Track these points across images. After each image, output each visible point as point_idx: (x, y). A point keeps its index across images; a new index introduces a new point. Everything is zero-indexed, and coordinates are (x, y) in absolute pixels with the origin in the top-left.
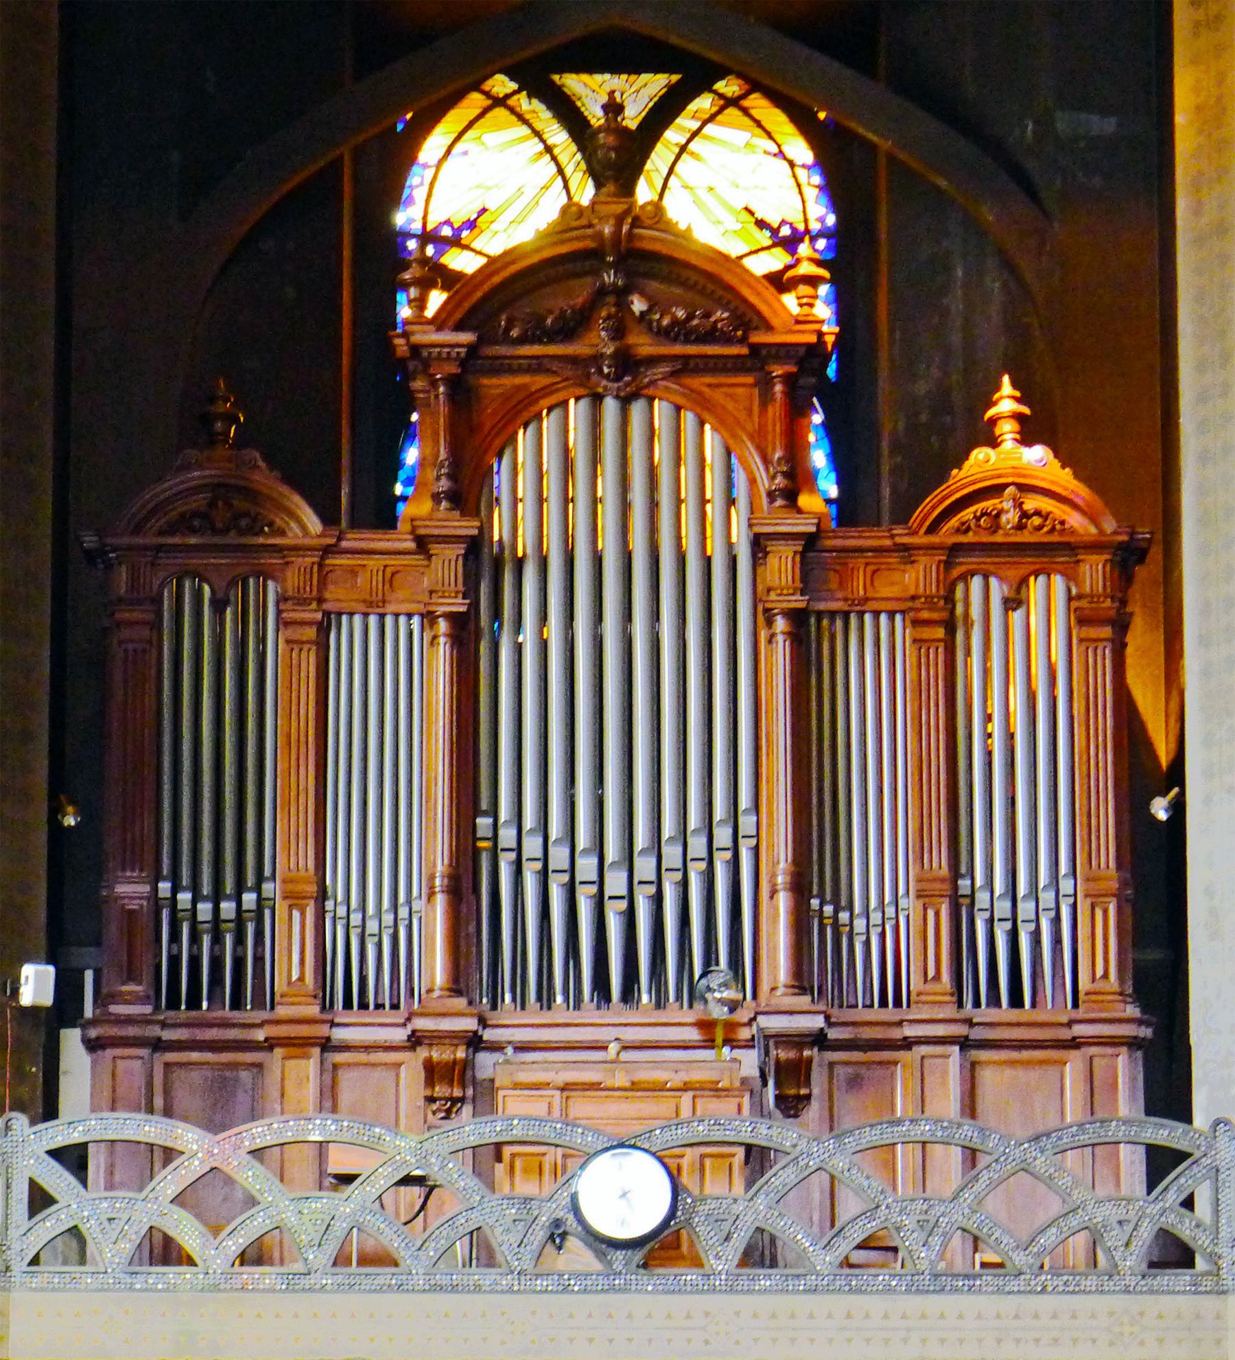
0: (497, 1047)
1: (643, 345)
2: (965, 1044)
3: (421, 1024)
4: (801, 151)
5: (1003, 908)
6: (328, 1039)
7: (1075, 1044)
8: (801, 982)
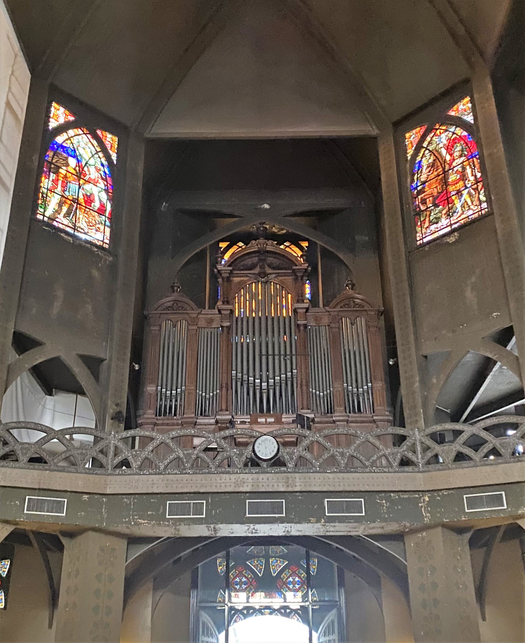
2: (347, 421)
3: (218, 417)
6: (196, 422)
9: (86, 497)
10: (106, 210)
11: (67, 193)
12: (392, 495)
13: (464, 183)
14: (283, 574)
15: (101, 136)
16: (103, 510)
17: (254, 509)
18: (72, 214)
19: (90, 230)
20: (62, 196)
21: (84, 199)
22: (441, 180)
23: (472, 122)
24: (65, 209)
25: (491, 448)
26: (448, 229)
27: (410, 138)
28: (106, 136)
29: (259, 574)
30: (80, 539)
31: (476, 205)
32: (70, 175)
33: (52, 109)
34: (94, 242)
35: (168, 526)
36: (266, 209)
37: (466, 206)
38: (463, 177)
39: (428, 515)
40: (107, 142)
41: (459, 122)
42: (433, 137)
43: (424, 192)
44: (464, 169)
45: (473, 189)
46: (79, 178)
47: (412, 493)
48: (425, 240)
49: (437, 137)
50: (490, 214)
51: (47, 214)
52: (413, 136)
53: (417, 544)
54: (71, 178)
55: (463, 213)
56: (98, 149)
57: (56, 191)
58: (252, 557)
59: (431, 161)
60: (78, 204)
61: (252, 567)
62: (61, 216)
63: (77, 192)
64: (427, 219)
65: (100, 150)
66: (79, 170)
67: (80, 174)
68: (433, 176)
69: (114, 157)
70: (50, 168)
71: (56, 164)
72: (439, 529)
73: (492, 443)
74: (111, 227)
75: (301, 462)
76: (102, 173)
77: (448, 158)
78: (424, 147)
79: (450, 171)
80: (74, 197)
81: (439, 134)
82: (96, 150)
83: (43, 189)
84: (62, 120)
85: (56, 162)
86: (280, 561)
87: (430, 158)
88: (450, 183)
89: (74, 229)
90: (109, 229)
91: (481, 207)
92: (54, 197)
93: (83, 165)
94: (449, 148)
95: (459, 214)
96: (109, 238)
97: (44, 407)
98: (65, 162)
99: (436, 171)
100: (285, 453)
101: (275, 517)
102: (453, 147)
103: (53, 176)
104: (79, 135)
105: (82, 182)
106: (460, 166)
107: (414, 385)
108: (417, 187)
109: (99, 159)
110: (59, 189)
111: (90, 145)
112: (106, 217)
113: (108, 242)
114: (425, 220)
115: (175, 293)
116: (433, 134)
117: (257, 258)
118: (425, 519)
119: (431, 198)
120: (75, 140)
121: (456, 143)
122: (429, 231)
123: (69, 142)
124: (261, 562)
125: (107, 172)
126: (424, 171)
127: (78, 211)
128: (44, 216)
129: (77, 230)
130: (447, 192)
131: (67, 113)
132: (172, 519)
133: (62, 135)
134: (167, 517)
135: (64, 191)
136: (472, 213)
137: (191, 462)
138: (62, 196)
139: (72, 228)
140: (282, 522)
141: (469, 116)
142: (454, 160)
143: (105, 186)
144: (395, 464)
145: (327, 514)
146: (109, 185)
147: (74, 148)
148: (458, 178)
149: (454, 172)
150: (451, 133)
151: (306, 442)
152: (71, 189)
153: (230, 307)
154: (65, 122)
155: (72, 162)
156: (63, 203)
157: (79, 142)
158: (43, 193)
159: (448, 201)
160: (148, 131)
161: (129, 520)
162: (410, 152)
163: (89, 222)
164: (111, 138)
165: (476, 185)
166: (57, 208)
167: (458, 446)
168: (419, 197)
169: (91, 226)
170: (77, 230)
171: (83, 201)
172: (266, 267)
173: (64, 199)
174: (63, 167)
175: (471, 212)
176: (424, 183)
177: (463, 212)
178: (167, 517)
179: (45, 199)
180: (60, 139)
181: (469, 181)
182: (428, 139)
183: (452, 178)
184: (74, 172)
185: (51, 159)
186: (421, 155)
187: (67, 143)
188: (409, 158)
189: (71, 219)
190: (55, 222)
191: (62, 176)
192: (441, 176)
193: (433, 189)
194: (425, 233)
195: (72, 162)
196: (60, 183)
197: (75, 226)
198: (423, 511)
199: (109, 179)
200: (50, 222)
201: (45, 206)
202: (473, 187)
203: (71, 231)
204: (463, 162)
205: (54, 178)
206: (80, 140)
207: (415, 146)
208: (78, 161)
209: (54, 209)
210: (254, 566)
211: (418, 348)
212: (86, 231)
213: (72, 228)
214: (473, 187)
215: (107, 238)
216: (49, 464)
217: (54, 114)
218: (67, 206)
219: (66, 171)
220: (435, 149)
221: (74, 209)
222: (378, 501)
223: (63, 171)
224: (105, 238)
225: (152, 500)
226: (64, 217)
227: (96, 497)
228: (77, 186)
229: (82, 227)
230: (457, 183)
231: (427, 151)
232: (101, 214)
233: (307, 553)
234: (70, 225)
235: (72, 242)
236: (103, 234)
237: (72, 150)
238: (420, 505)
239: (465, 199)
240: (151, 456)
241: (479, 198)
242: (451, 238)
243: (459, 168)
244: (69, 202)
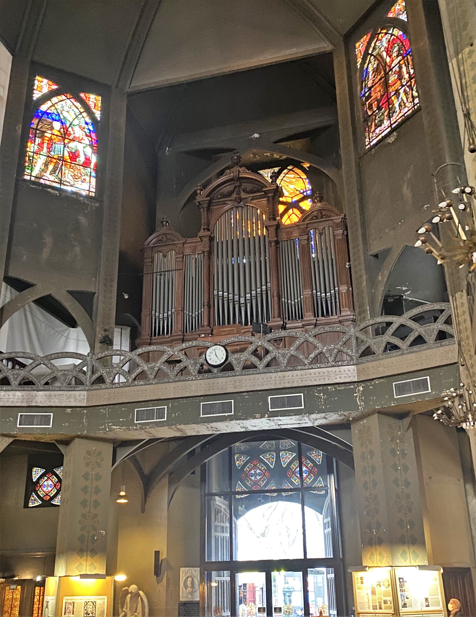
4: (304, 176)
9: (69, 410)
10: (90, 163)
11: (52, 153)
12: (329, 387)
13: (401, 82)
14: (292, 465)
15: (85, 98)
16: (84, 420)
17: (208, 409)
18: (58, 171)
19: (76, 182)
20: (48, 156)
21: (69, 156)
22: (383, 82)
23: (406, 20)
24: (51, 167)
25: (416, 336)
27: (359, 47)
28: (90, 98)
29: (271, 466)
30: (72, 446)
31: (410, 102)
32: (55, 137)
33: (36, 82)
34: (80, 192)
35: (136, 429)
36: (256, 138)
37: (402, 104)
38: (400, 77)
39: (362, 403)
40: (90, 103)
41: (396, 23)
42: (376, 42)
43: (372, 97)
44: (400, 68)
45: (408, 86)
46: (64, 138)
47: (348, 384)
48: (372, 144)
49: (379, 42)
50: (419, 109)
51: (34, 174)
52: (362, 44)
53: (360, 431)
54: (56, 139)
55: (400, 112)
56: (82, 110)
57: (42, 153)
58: (264, 451)
59: (375, 66)
60: (63, 161)
61: (265, 460)
63: (62, 151)
64: (373, 123)
65: (84, 110)
66: (64, 131)
68: (377, 80)
69: (98, 115)
70: (36, 133)
71: (41, 129)
72: (376, 415)
73: (417, 331)
74: (96, 177)
76: (87, 131)
77: (388, 60)
78: (370, 54)
79: (390, 73)
80: (60, 155)
81: (381, 38)
82: (80, 112)
83: (29, 153)
84: (45, 90)
85: (41, 128)
86: (289, 454)
87: (374, 64)
88: (390, 84)
89: (61, 184)
90: (95, 179)
91: (414, 103)
92: (40, 158)
93: (68, 127)
95: (397, 113)
96: (94, 187)
97: (67, 338)
98: (50, 126)
99: (380, 75)
100: (233, 359)
101: (225, 416)
102: (392, 47)
103: (38, 140)
104: (63, 100)
105: (66, 141)
106: (398, 65)
107: (362, 283)
109: (83, 119)
110: (45, 150)
111: (73, 108)
112: (91, 168)
113: (94, 190)
114: (371, 124)
115: (165, 227)
116: (376, 39)
117: (233, 185)
118: (360, 408)
119: (376, 103)
120: (59, 106)
121: (394, 44)
122: (374, 135)
123: (53, 108)
124: (272, 455)
125: (92, 129)
126: (370, 77)
127: (63, 167)
128: (31, 176)
129: (63, 184)
130: (387, 94)
131: (50, 83)
132: (139, 424)
133: (46, 103)
134: (135, 422)
135: (49, 152)
136: (407, 111)
137: (154, 374)
139: (58, 183)
140: (231, 420)
141: (404, 14)
142: (393, 61)
145: (270, 410)
146: (93, 140)
147: (58, 112)
148: (396, 78)
149: (393, 73)
150: (390, 35)
151: (251, 348)
152: (56, 150)
154: (49, 91)
156: (49, 163)
157: (63, 107)
158: (29, 157)
159: (389, 102)
160: (128, 86)
161: (105, 426)
162: (359, 60)
163: (75, 175)
164: (95, 98)
165: (409, 83)
166: (43, 168)
167: (388, 337)
168: (367, 103)
169: (77, 179)
170: (63, 184)
171: (68, 157)
172: (242, 192)
173: (50, 159)
174: (48, 131)
175: (406, 109)
176: (370, 89)
177: (401, 110)
178: (135, 422)
179: (31, 162)
180: (44, 108)
181: (405, 79)
182: (373, 45)
183: (393, 78)
184: (58, 133)
185: (36, 126)
186: (367, 61)
187: (51, 110)
188: (359, 67)
189: (57, 176)
190: (41, 180)
191: (47, 139)
192: (383, 79)
193: (377, 93)
194: (372, 137)
195: (57, 125)
196: (45, 145)
197: (61, 180)
198: (358, 400)
199: (93, 135)
200: (37, 180)
201: (32, 167)
202: (408, 84)
203: (58, 186)
204: (400, 61)
205: (40, 142)
206: (64, 105)
207: (363, 54)
208: (62, 123)
209: (40, 168)
210: (266, 459)
211: (366, 250)
212: (72, 183)
213: (58, 183)
214: (408, 84)
215: (93, 187)
216: (36, 386)
217: (38, 86)
218: (53, 164)
219: (52, 134)
220: (378, 53)
221: (59, 167)
222: (317, 394)
223: (48, 135)
224: (91, 187)
225: (123, 409)
226: (51, 174)
227: (78, 409)
228: (63, 146)
229: (68, 180)
230: (395, 84)
231: (372, 57)
232: (86, 167)
233: (299, 446)
234: (56, 180)
235: (58, 195)
236: (89, 184)
237: (56, 115)
238: (355, 395)
239: (401, 98)
241: (412, 94)
242: (391, 138)
243: (397, 68)
244: (55, 161)
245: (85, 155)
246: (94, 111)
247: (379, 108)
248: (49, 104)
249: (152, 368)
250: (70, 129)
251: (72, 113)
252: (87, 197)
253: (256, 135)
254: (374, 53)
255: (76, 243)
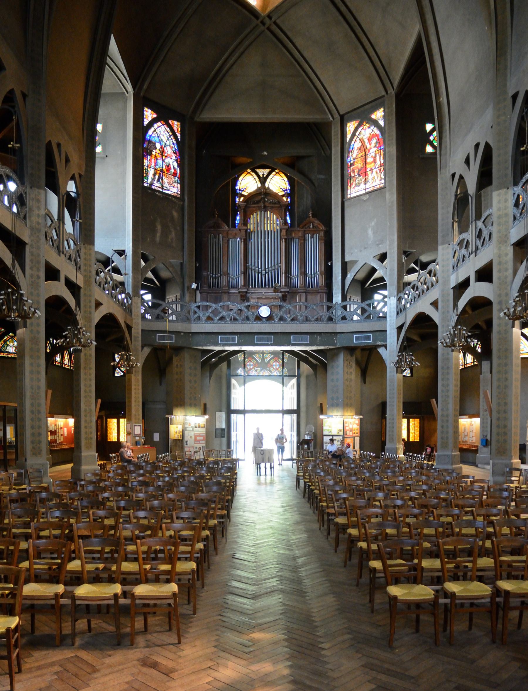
0: (249, 293)
1: (267, 204)
2: (306, 293)
5: (310, 276)
7: (319, 293)
8: (286, 285)
10: (177, 173)
11: (157, 167)
17: (259, 340)
23: (383, 126)
24: (157, 177)
26: (364, 192)
33: (145, 112)
38: (375, 161)
41: (375, 123)
44: (376, 155)
46: (162, 156)
50: (385, 187)
51: (149, 182)
56: (171, 134)
62: (155, 182)
67: (162, 153)
69: (179, 138)
75: (281, 319)
76: (174, 150)
77: (368, 146)
84: (150, 119)
89: (163, 189)
94: (370, 140)
102: (371, 139)
103: (149, 157)
104: (160, 126)
108: (350, 161)
113: (179, 193)
131: (153, 112)
135: (156, 165)
138: (155, 169)
142: (371, 148)
143: (176, 157)
144: (325, 320)
153: (245, 228)
155: (158, 146)
159: (366, 174)
163: (169, 182)
176: (354, 159)
180: (150, 132)
193: (359, 164)
196: (153, 161)
197: (162, 186)
199: (177, 152)
203: (161, 190)
223: (154, 153)
231: (358, 139)
234: (160, 186)
240: (211, 315)
243: (373, 155)
244: (158, 172)
245: (174, 167)
246: (177, 134)
247: (359, 175)
248: (152, 129)
249: (229, 314)
250: (165, 149)
251: (165, 136)
252: (175, 197)
253: (265, 153)
254: (360, 137)
255: (173, 230)
